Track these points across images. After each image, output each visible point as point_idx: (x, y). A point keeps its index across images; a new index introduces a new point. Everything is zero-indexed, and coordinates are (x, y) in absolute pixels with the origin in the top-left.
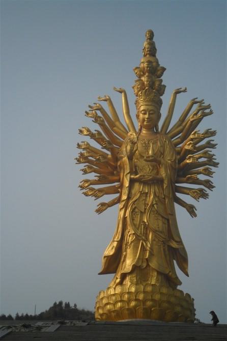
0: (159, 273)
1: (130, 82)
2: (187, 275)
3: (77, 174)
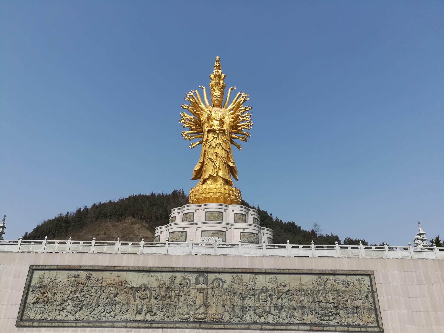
0: (223, 179)
2: (237, 180)
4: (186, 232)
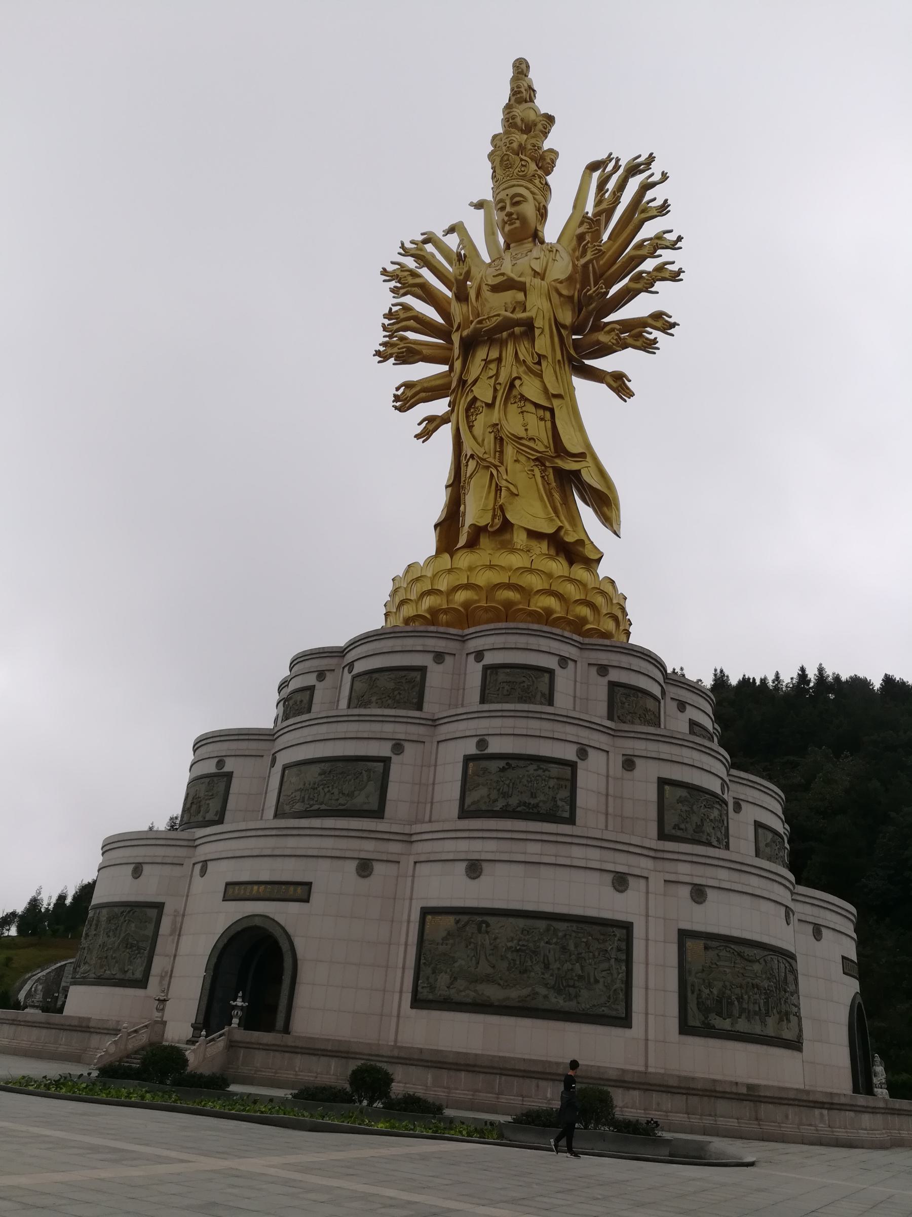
4: (229, 776)
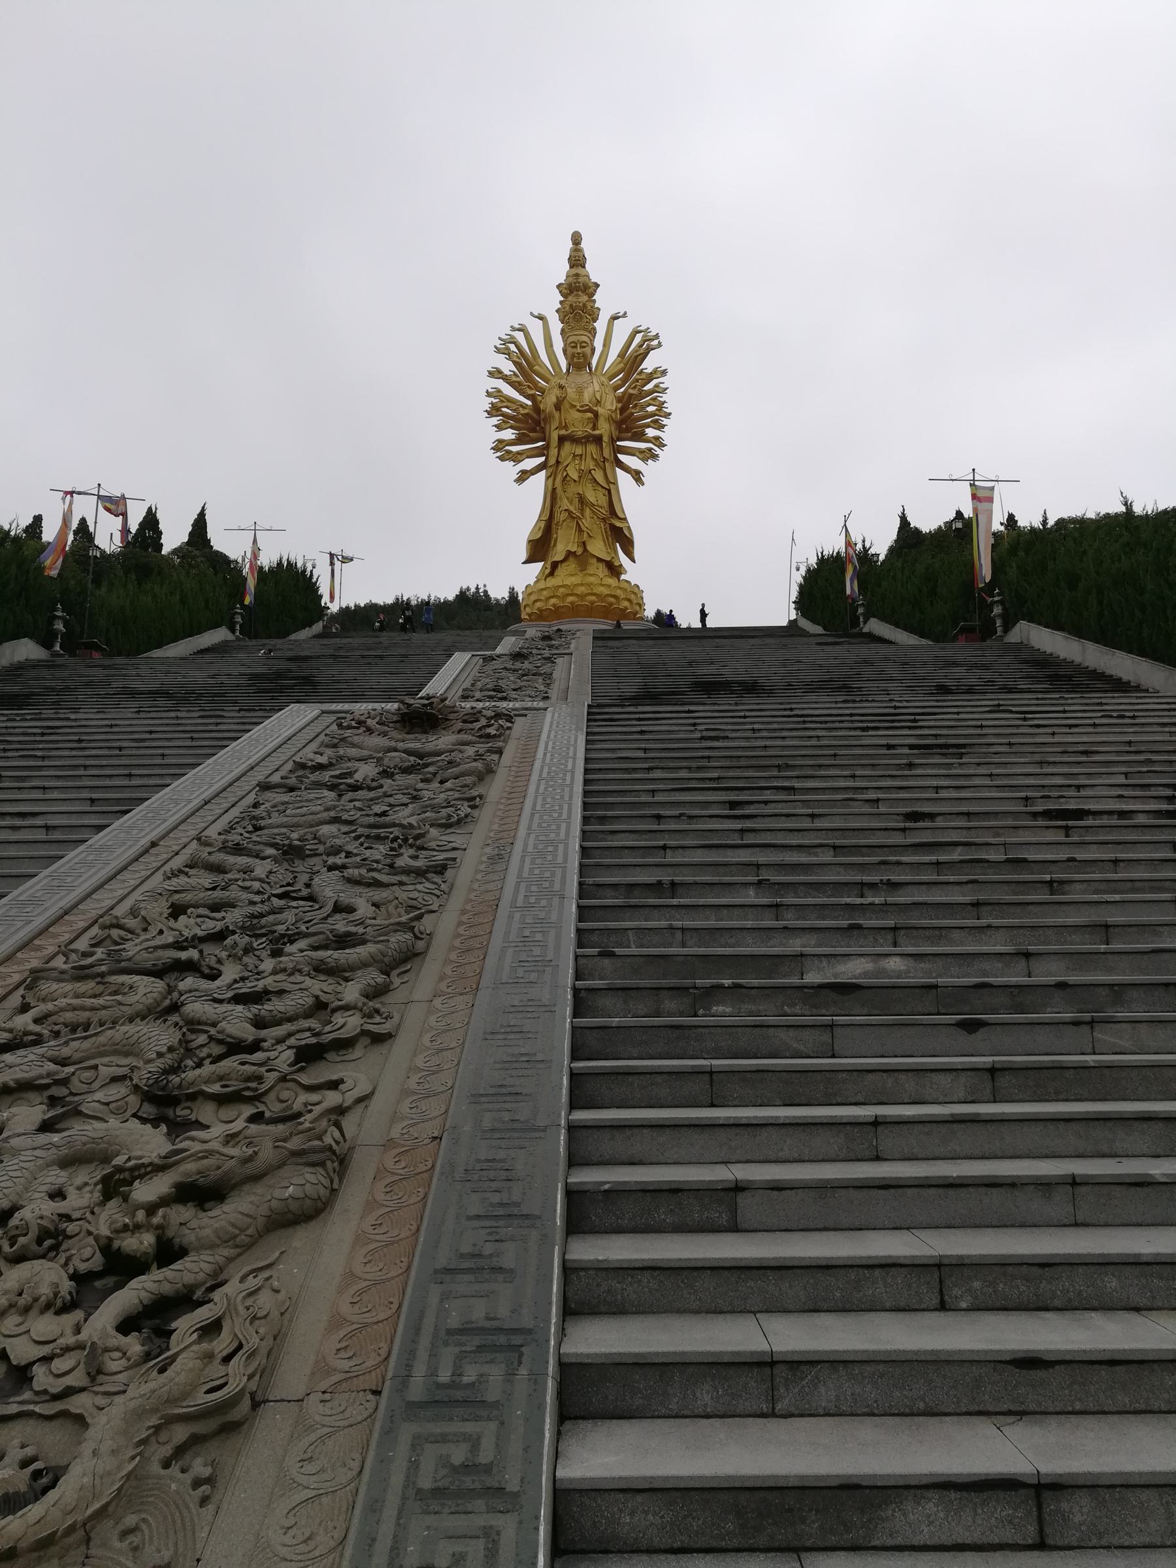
1: (550, 303)
3: (488, 431)
